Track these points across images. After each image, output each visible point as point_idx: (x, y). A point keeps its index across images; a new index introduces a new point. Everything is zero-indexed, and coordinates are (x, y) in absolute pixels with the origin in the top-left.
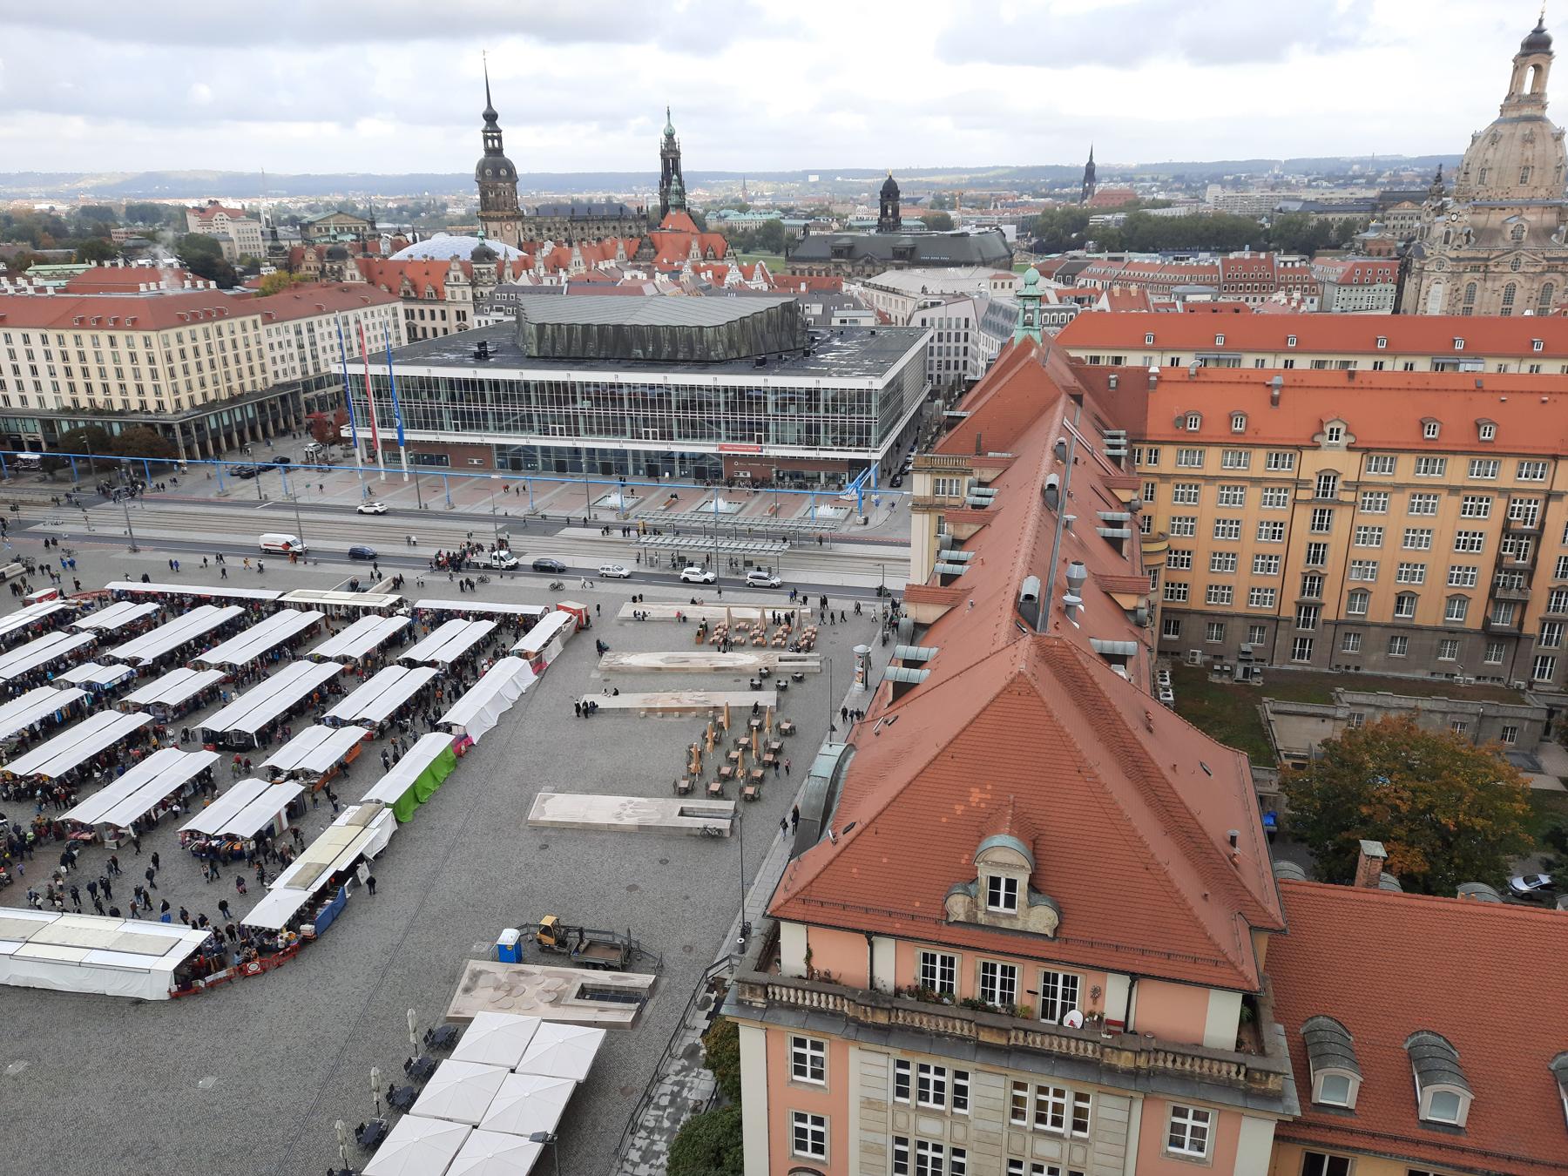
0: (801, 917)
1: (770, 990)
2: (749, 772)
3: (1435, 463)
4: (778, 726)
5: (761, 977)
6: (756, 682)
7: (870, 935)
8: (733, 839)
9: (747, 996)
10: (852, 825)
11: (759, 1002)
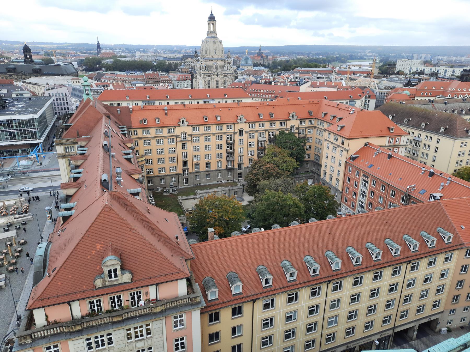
0: (41, 306)
1: (33, 335)
2: (9, 262)
3: (196, 128)
4: (19, 242)
5: (28, 332)
6: (6, 229)
7: (69, 303)
8: (7, 288)
9: (23, 341)
10: (55, 269)
11: (29, 341)
